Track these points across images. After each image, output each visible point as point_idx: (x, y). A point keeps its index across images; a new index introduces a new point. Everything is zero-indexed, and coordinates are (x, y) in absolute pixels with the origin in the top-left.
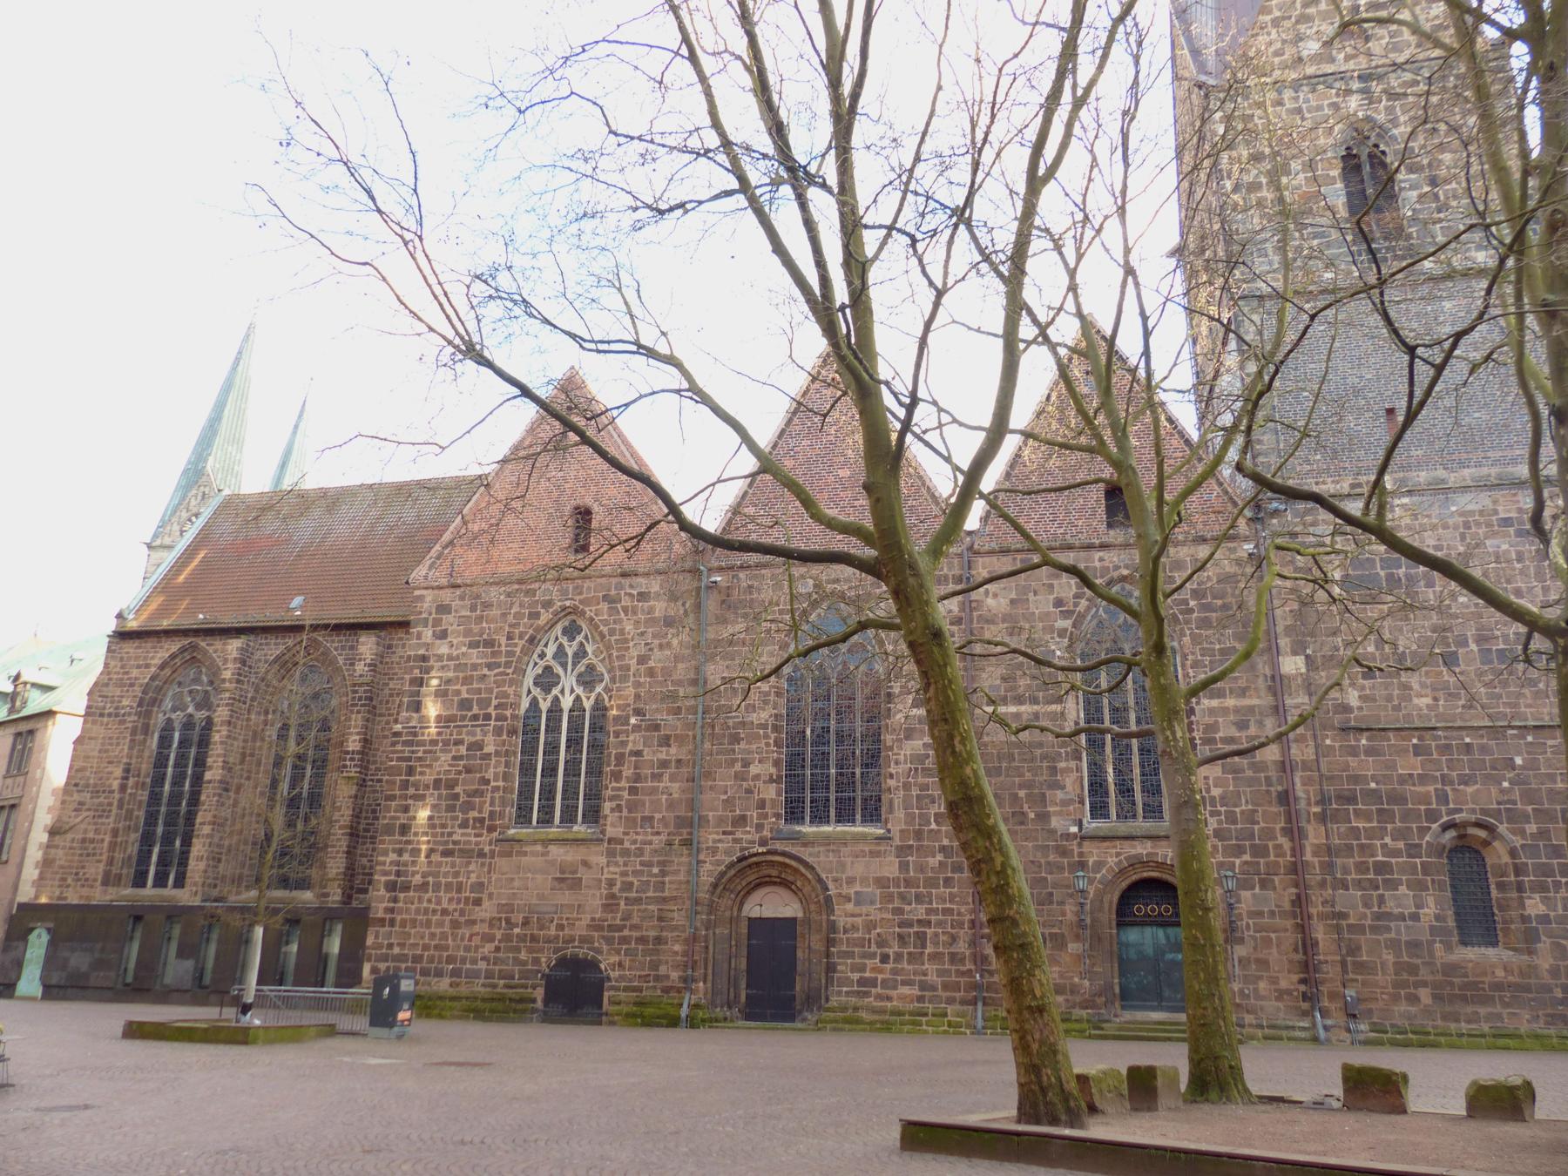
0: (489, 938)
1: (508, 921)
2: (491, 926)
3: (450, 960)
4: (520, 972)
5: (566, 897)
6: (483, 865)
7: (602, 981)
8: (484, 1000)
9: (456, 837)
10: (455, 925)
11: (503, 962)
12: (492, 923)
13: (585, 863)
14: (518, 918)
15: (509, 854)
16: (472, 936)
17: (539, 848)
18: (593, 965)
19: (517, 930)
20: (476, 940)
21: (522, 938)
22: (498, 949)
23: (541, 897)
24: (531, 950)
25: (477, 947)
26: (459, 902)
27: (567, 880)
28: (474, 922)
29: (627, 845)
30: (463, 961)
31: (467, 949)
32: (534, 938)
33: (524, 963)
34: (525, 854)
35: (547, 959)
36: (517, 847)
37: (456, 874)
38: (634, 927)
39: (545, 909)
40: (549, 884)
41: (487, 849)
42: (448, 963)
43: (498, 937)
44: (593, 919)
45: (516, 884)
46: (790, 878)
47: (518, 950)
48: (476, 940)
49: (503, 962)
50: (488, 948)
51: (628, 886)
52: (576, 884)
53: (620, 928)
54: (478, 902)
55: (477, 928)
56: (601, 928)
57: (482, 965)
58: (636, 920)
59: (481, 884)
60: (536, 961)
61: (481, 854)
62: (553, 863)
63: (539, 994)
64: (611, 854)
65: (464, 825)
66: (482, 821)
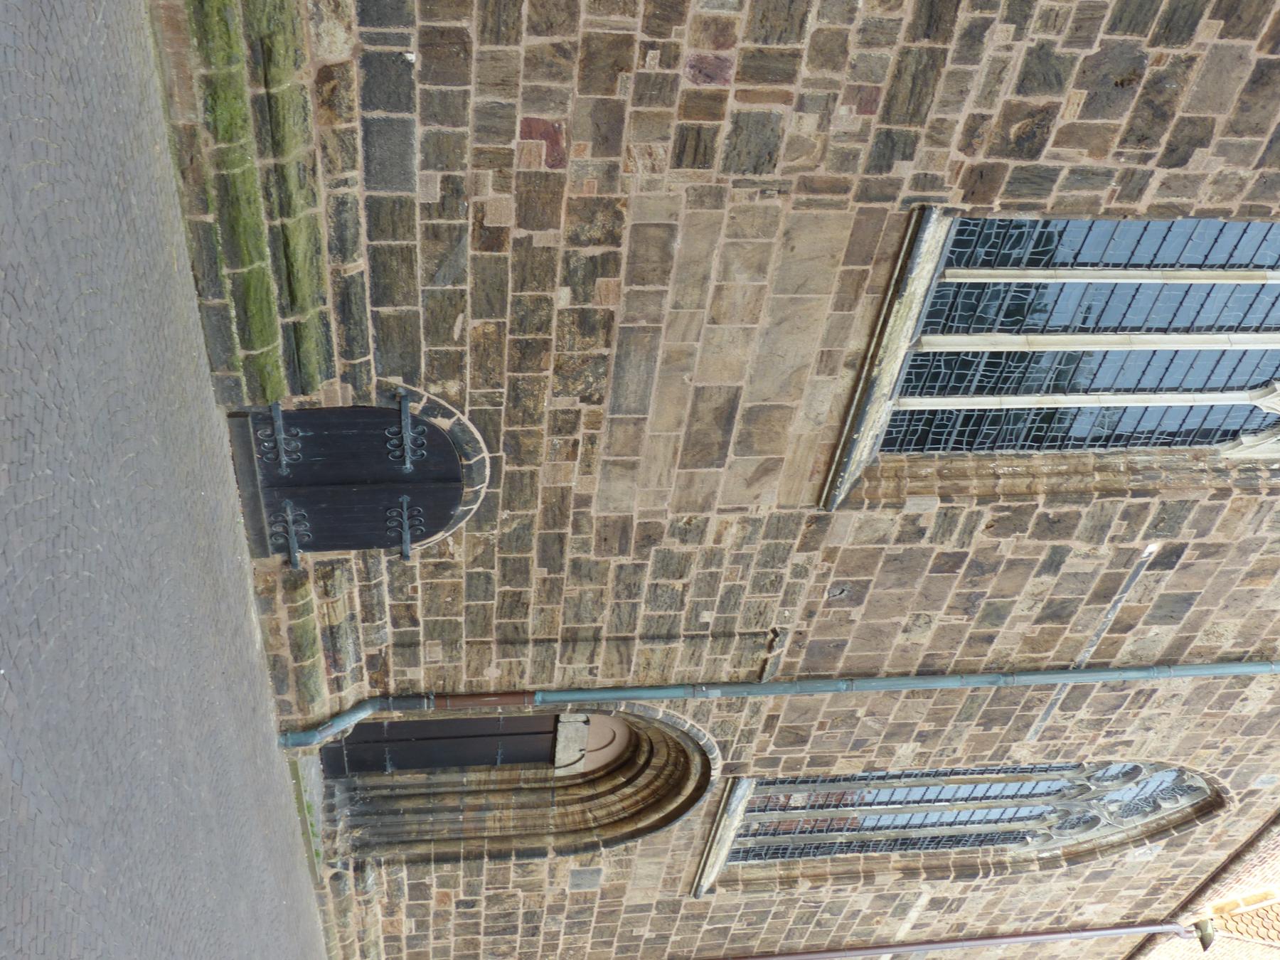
0: (537, 202)
1: (604, 266)
2: (586, 209)
3: (445, 49)
4: (405, 322)
5: (664, 424)
6: (847, 159)
7: (392, 542)
8: (281, 240)
9: (1000, 33)
10: (604, 60)
11: (443, 264)
12: (603, 210)
13: (766, 470)
14: (611, 295)
15: (858, 251)
16: (551, 134)
17: (855, 343)
18: (440, 520)
19: (562, 297)
20: (530, 156)
21: (533, 316)
22: (492, 238)
23: (678, 362)
24: (485, 349)
25: (502, 161)
26: (704, 70)
27: (723, 427)
28: (608, 137)
29: (798, 558)
30: (444, 110)
31: (494, 122)
32: (528, 353)
33: (439, 326)
34: (845, 303)
35: (450, 401)
36: (878, 274)
37: (830, 51)
38: (552, 590)
39: (632, 379)
40: (720, 380)
41: (905, 170)
42: (430, 41)
43: (541, 238)
44: (584, 501)
45: (741, 280)
46: (641, 781)
47: (489, 304)
48: (530, 156)
49: (443, 264)
50: (501, 208)
51: (673, 566)
52: (702, 451)
53: (551, 558)
54: (692, 150)
55: (582, 163)
56: (556, 513)
57: (425, 187)
58: (571, 589)
59: (764, 160)
60: (449, 366)
61: (890, 149)
62: (792, 383)
63: (332, 393)
64: (780, 526)
65: (1042, 71)
66: (1029, 144)
